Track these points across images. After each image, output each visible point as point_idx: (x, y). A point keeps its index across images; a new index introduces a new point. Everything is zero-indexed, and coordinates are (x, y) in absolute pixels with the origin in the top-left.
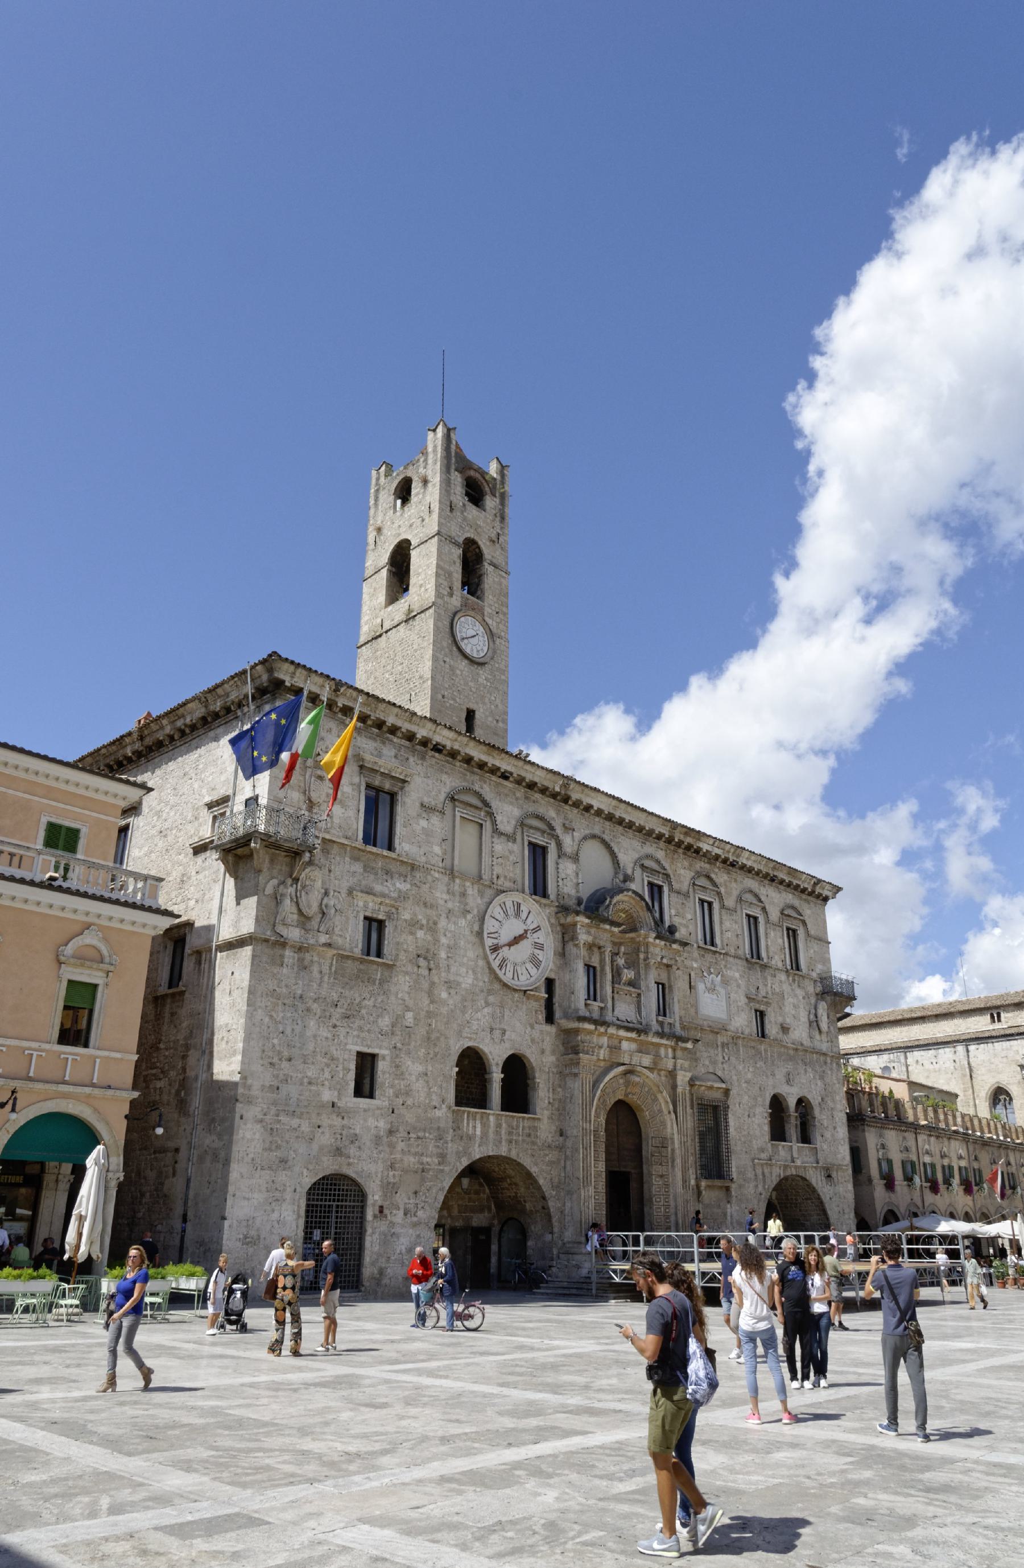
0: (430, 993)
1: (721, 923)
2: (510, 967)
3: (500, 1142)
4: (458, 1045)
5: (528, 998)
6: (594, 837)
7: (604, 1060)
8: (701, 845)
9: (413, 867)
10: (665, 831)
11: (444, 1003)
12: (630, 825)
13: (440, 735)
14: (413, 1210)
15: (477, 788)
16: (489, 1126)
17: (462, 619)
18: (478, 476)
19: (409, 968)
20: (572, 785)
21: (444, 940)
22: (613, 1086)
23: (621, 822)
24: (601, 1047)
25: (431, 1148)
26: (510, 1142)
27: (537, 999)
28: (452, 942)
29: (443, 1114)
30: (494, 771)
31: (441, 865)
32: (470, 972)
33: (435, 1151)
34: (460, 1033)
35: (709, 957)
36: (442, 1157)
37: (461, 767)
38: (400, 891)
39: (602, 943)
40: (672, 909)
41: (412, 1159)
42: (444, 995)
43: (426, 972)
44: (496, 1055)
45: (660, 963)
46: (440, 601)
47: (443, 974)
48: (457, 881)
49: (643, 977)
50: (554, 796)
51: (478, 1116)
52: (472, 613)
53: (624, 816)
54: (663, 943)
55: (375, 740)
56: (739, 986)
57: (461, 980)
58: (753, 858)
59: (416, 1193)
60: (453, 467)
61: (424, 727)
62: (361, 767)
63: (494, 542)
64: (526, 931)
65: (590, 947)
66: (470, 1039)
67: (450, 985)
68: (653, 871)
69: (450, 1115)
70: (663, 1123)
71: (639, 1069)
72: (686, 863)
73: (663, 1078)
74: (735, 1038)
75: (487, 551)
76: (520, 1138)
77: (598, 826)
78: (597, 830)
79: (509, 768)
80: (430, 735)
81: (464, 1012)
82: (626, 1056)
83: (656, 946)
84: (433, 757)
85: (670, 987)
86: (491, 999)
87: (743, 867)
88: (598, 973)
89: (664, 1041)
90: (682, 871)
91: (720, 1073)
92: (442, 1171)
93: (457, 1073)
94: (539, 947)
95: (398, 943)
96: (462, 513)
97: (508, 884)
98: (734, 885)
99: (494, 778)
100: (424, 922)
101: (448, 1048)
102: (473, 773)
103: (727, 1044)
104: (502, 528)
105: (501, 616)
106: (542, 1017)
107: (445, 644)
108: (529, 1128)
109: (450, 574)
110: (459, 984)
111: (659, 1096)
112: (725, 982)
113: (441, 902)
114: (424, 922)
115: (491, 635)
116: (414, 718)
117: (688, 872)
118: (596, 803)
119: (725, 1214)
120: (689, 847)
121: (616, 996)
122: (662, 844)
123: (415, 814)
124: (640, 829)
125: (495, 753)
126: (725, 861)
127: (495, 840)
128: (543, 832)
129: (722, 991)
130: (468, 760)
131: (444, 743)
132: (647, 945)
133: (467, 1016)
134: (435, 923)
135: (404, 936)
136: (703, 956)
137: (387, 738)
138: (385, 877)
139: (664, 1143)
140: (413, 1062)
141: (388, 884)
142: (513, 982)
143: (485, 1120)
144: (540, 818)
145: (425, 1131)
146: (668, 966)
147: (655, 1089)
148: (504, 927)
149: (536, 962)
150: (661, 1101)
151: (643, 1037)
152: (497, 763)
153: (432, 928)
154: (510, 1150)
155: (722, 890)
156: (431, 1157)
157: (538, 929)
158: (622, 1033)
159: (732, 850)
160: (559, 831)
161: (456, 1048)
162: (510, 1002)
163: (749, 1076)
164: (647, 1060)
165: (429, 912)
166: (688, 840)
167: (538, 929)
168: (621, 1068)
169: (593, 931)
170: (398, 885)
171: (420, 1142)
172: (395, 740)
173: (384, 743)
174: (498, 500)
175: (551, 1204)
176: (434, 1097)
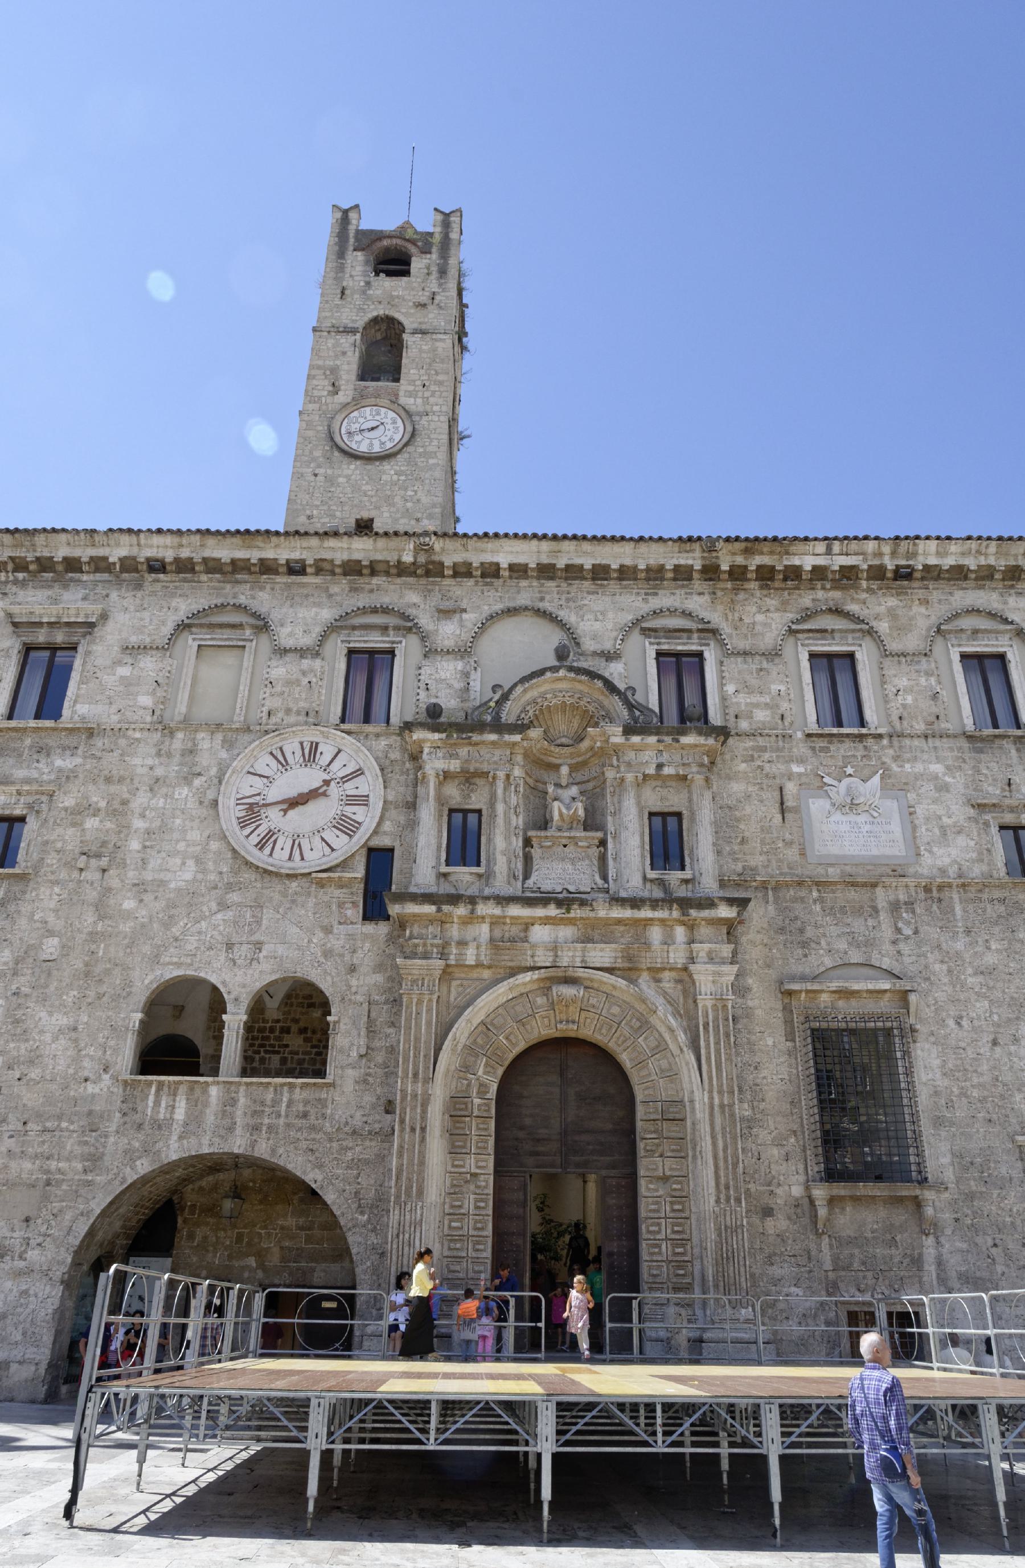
0: (100, 908)
1: (883, 680)
2: (284, 843)
3: (231, 1129)
4: (150, 977)
5: (322, 887)
6: (511, 612)
7: (479, 965)
8: (796, 561)
9: (90, 733)
10: (694, 559)
11: (127, 915)
12: (600, 573)
13: (151, 546)
14: (18, 1249)
15: (242, 600)
16: (206, 1104)
17: (355, 414)
18: (395, 241)
19: (63, 875)
20: (438, 544)
21: (139, 824)
22: (499, 1013)
23: (573, 572)
24: (462, 943)
25: (70, 1144)
26: (256, 1128)
27: (341, 885)
28: (158, 823)
29: (103, 1089)
30: (267, 567)
31: (149, 719)
32: (191, 863)
33: (78, 1150)
34: (155, 959)
35: (845, 749)
36: (94, 1161)
37: (211, 580)
38: (60, 770)
39: (485, 767)
40: (722, 686)
41: (27, 1165)
42: (129, 904)
43: (98, 875)
44: (240, 984)
45: (658, 776)
46: (311, 407)
47: (131, 874)
48: (180, 735)
49: (611, 809)
50: (402, 570)
51: (183, 1089)
52: (372, 401)
53: (577, 561)
54: (652, 739)
55: (50, 587)
56: (943, 788)
57: (168, 876)
58: (953, 547)
59: (27, 1220)
60: (351, 248)
61: (118, 545)
62: (15, 625)
63: (424, 306)
64: (327, 783)
65: (469, 777)
66: (178, 965)
67: (140, 888)
68: (673, 633)
69: (118, 1090)
70: (672, 1075)
71: (581, 973)
72: (772, 602)
73: (667, 985)
74: (935, 890)
75: (408, 323)
76: (282, 1121)
77: (526, 593)
78: (524, 599)
79: (296, 555)
80: (135, 551)
81: (167, 926)
82: (540, 952)
83: (638, 749)
84: (158, 581)
85: (693, 813)
86: (234, 897)
87: (933, 573)
88: (484, 819)
89: (646, 913)
90: (765, 617)
91: (886, 963)
92: (89, 1183)
93: (142, 1022)
94: (362, 800)
95: (46, 843)
96: (364, 292)
97: (292, 719)
98: (918, 610)
99: (279, 579)
100: (103, 804)
101: (130, 984)
102: (237, 582)
103: (910, 904)
104: (440, 285)
105: (433, 388)
106: (355, 913)
107: (318, 453)
108: (306, 1102)
109: (334, 370)
110: (162, 883)
111: (653, 1020)
112: (893, 786)
113: (145, 770)
114: (103, 804)
115: (407, 414)
116: (97, 538)
117: (776, 615)
118: (504, 555)
119: (917, 1262)
120: (766, 575)
121: (536, 852)
122: (697, 584)
123: (108, 662)
124: (626, 574)
125: (259, 541)
126: (877, 573)
127: (274, 663)
128: (384, 629)
129: (891, 806)
130: (213, 566)
131: (160, 555)
132: (617, 750)
133: (176, 931)
134: (125, 803)
135: (59, 830)
136: (826, 750)
137: (72, 580)
138: (35, 757)
139: (674, 1114)
140: (50, 1014)
141: (40, 765)
142: (290, 864)
143: (198, 1091)
144: (386, 610)
145: (60, 1118)
146: (684, 778)
147: (641, 1007)
148: (276, 783)
149: (346, 826)
150: (663, 1029)
151: (576, 912)
152: (269, 554)
153: (119, 810)
154: (253, 1144)
155: (883, 627)
156: (68, 1160)
157: (359, 772)
158: (516, 911)
159: (886, 549)
160: (425, 620)
161: (146, 981)
162: (277, 897)
163: (990, 959)
164: (602, 954)
165: (113, 789)
166: (758, 560)
167: (359, 772)
168: (528, 977)
169: (463, 752)
170: (59, 763)
171: (47, 1136)
172: (85, 577)
173: (66, 587)
174: (434, 256)
175: (354, 1240)
176: (86, 1063)
